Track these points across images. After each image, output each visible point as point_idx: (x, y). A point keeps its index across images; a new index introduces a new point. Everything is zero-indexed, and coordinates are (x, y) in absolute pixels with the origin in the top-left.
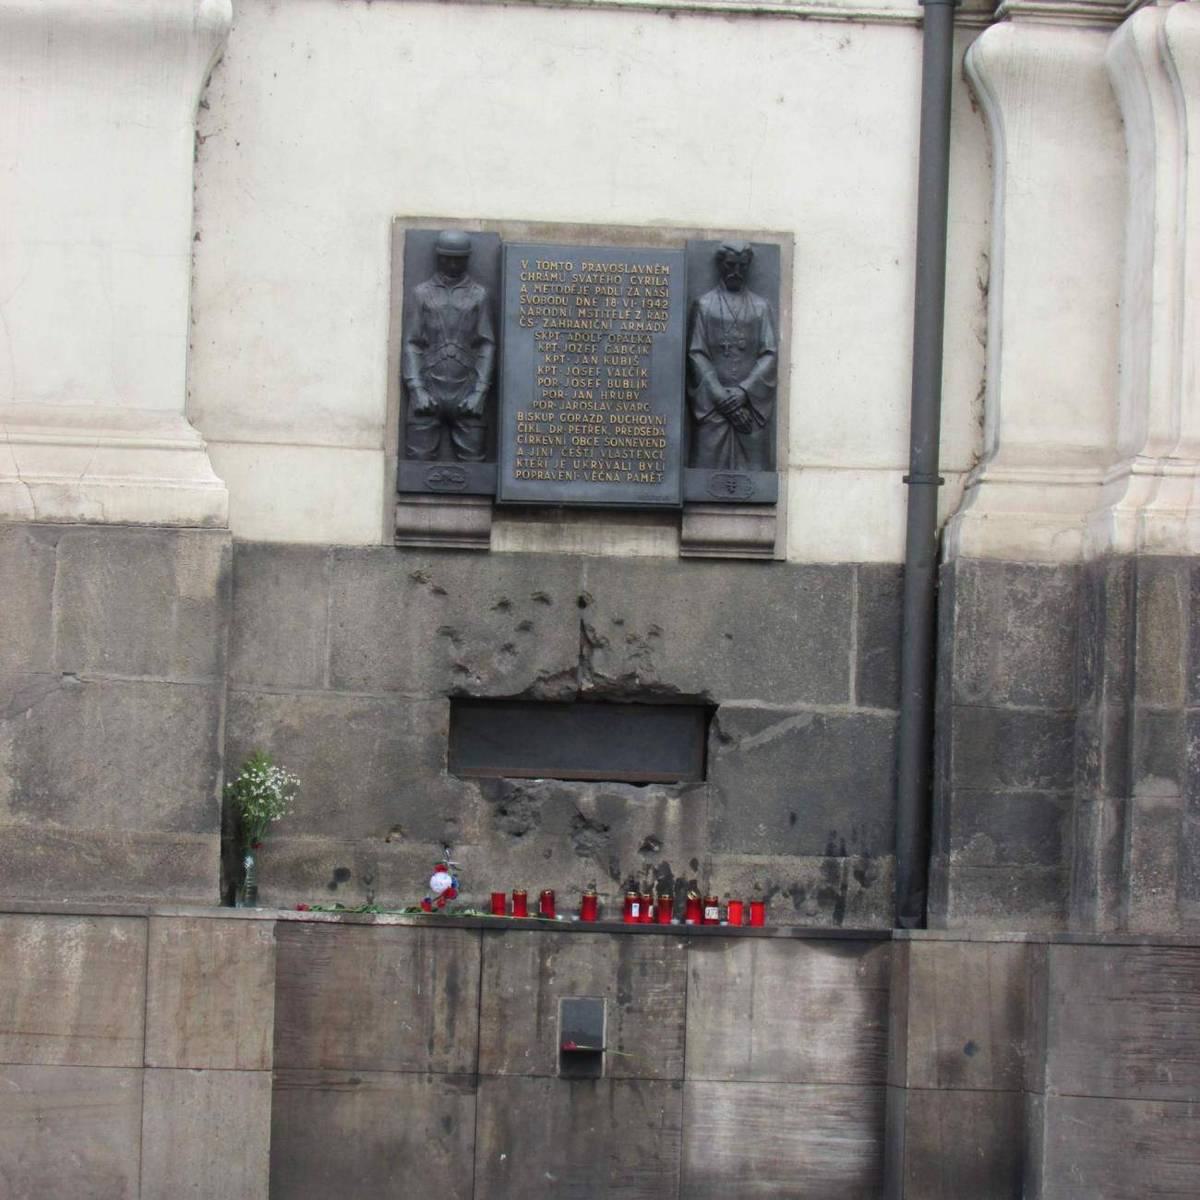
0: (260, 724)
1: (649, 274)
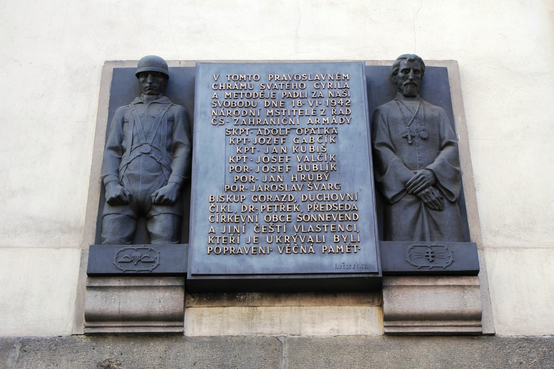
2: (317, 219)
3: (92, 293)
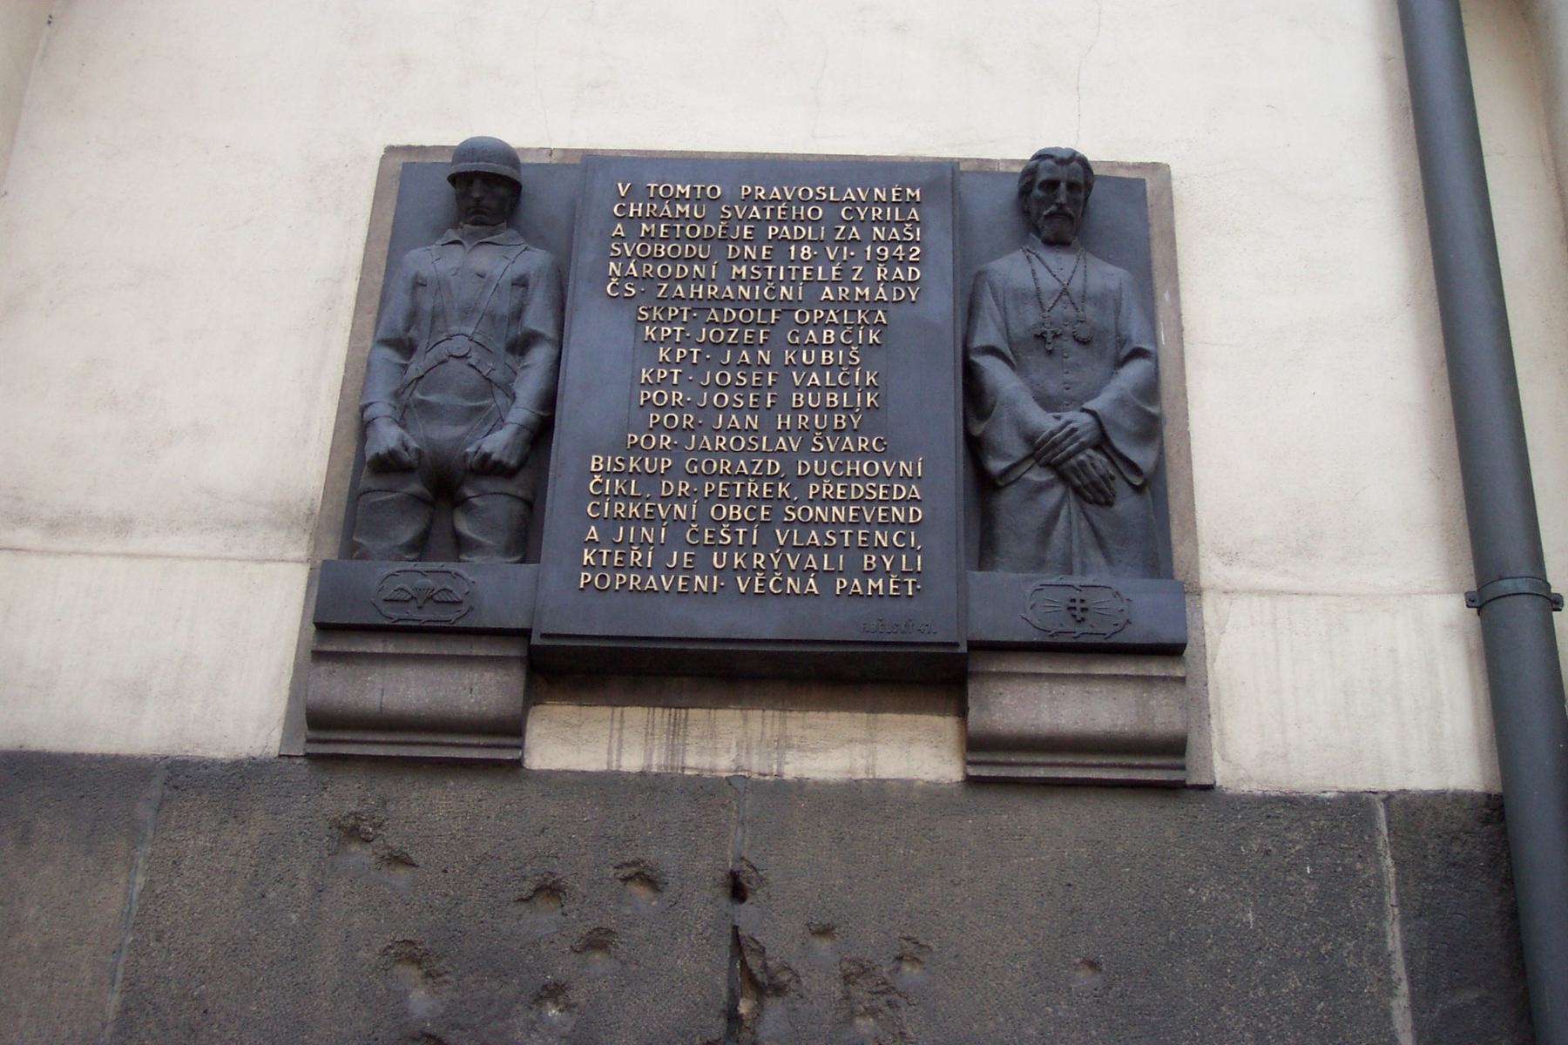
1: (879, 202)
2: (830, 517)
3: (324, 668)
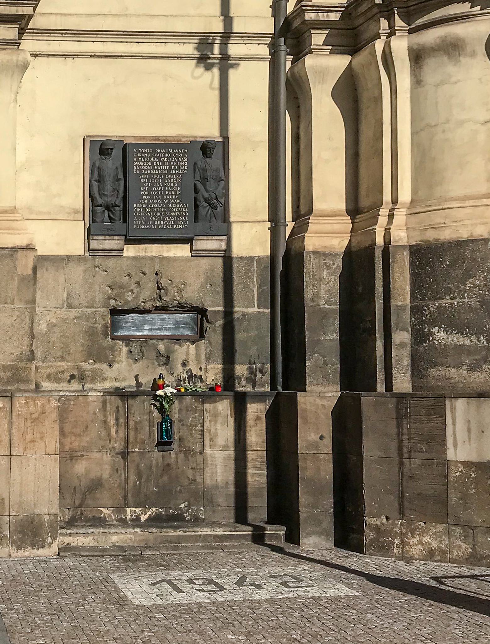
0: (42, 322)
1: (180, 153)
